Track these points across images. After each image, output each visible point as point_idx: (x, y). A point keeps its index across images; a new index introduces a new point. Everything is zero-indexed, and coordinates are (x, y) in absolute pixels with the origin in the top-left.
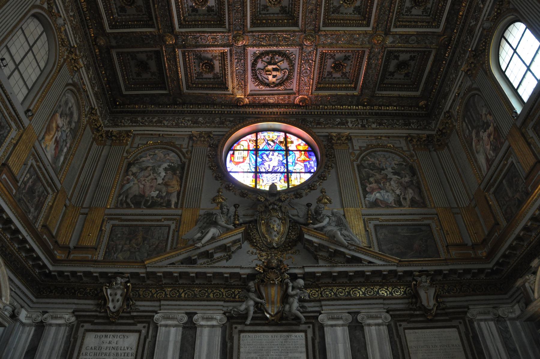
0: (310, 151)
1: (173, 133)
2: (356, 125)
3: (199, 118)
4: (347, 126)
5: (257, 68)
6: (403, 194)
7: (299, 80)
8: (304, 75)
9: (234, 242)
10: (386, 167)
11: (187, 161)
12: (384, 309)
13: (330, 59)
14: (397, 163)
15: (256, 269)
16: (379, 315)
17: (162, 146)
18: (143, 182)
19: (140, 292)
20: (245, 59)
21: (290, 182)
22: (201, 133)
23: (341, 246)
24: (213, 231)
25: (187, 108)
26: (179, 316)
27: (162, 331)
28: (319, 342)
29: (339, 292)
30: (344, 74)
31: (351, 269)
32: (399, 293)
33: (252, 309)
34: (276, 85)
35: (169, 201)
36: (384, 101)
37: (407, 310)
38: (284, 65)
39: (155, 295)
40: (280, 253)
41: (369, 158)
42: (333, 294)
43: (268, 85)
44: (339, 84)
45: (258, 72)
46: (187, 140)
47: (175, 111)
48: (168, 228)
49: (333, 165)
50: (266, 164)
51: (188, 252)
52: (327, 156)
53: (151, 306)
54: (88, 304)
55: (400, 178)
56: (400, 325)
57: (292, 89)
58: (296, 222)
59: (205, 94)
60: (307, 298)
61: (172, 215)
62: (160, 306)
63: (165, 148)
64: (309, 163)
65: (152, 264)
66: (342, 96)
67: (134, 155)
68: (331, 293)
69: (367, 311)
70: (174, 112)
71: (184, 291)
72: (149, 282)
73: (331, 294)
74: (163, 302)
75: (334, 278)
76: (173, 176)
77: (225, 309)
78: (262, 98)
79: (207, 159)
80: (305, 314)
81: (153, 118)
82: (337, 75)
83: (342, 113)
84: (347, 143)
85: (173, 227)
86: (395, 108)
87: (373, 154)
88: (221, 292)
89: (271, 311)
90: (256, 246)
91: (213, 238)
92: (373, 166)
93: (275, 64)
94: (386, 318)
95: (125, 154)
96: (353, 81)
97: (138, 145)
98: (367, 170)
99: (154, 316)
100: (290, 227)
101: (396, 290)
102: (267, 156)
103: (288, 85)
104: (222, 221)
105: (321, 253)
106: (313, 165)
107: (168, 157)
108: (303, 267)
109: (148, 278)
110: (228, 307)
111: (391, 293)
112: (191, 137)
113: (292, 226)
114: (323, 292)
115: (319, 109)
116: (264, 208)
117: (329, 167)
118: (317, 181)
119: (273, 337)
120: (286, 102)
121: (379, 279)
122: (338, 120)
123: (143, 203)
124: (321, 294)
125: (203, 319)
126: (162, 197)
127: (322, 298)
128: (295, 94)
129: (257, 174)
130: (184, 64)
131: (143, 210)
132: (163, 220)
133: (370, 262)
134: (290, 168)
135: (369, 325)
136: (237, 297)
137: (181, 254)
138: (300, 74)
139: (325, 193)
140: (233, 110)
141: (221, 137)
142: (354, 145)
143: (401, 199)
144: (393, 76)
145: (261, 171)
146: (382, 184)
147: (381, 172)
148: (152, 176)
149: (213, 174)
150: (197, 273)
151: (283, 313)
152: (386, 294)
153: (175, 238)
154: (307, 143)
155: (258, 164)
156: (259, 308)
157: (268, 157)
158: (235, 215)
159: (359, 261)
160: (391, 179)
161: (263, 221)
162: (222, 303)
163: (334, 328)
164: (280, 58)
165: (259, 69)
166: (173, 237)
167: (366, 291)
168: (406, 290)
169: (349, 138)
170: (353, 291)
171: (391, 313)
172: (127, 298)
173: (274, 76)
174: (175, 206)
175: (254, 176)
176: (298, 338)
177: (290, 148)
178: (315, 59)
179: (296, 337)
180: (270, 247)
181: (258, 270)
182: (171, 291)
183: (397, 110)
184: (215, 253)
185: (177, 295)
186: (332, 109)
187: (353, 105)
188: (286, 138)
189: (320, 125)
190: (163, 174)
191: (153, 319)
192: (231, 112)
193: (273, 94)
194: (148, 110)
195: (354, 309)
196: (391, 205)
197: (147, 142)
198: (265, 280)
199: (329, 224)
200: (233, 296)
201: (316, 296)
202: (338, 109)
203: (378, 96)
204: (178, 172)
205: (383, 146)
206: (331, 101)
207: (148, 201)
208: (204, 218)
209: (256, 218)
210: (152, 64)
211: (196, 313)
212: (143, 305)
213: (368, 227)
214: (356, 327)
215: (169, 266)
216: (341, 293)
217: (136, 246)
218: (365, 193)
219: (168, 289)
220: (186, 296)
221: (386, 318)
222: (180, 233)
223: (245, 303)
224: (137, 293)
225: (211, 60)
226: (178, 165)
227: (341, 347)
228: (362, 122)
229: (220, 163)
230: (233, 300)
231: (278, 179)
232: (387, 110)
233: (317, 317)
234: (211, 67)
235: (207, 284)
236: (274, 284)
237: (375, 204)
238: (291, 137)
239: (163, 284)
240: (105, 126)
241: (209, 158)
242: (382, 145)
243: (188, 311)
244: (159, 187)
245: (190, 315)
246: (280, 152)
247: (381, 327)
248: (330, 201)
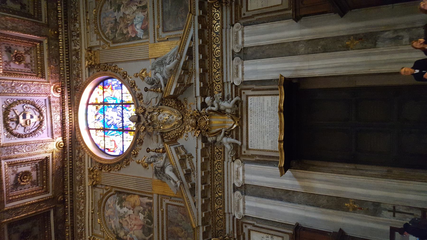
1: (91, 201)
2: (78, 41)
3: (77, 180)
4: (79, 50)
5: (23, 133)
6: (136, 4)
7: (35, 94)
8: (28, 90)
9: (178, 152)
10: (114, 18)
11: (114, 189)
12: (230, 28)
13: (10, 65)
14: (109, 7)
15: (197, 136)
16: (235, 33)
17: (102, 210)
18: (132, 226)
19: (219, 230)
20: (14, 145)
21: (130, 102)
22: (90, 178)
23: (179, 64)
24: (168, 171)
25: (67, 191)
26: (236, 198)
27: (248, 213)
28: (256, 85)
29: (217, 67)
30: (27, 52)
32: (218, 14)
33: (230, 140)
34: (41, 114)
35: (147, 204)
36: (52, 15)
37: (232, 8)
38: (19, 109)
39: (221, 217)
40: (186, 114)
41: (107, 32)
42: (218, 72)
43: (41, 122)
44: (37, 57)
45: (28, 132)
46: (97, 190)
47: (70, 200)
48: (168, 205)
49: (113, 65)
50: (116, 121)
51: (185, 191)
52: (107, 70)
53: (229, 220)
55: (122, 6)
56: (244, 14)
57: (45, 100)
58: (162, 100)
59: (52, 177)
60: (221, 94)
61: (158, 202)
62: (229, 213)
63: (104, 207)
64: (114, 85)
65: (196, 221)
66: (49, 55)
67: (110, 235)
68: (217, 74)
69: (232, 44)
70: (72, 201)
71: (217, 193)
72: (210, 222)
73: (218, 74)
74: (226, 211)
75: (205, 71)
76: (128, 201)
77: (230, 160)
78: (56, 126)
79: (112, 172)
80: (234, 96)
81: (78, 219)
82: (28, 59)
83: (67, 54)
84: (94, 52)
85: (167, 201)
86: (59, 4)
87: (103, 28)
88: (217, 163)
89: (231, 124)
90: (181, 133)
91: (174, 171)
92: (114, 29)
93: (18, 117)
94: (238, 27)
96: (33, 44)
97: (102, 231)
98: (116, 35)
99: (237, 219)
100: (165, 105)
101: (215, 17)
102: (109, 120)
103: (39, 104)
104: (160, 162)
105: (186, 81)
106: (115, 82)
107: (111, 205)
108: (196, 97)
109: (208, 223)
110: (228, 158)
111: (218, 21)
112: (94, 186)
113: (165, 103)
114: (216, 80)
115: (64, 75)
116: (150, 127)
117: (115, 69)
118: (128, 79)
119: (251, 122)
120: (59, 104)
121: (206, 31)
122: (74, 58)
123: (149, 226)
124: (218, 82)
125: (238, 178)
126: (144, 210)
127: (221, 81)
128: (49, 97)
129: (124, 130)
130: (22, 200)
131: (154, 226)
132: (162, 210)
133: (192, 40)
134: (119, 102)
135: (243, 42)
136: (221, 150)
137: (187, 197)
138: (27, 94)
139: (137, 73)
140: (68, 151)
141: (93, 161)
142: (95, 45)
143: (140, 5)
144: (25, 5)
145: (121, 126)
146: (129, 22)
147: (118, 23)
148: (127, 218)
149: (124, 167)
150: (202, 184)
151: (232, 114)
152: (219, 26)
153: (177, 199)
154: (97, 86)
155: (116, 129)
156: (229, 133)
157: (110, 120)
158: (155, 152)
160: (124, 13)
161: (161, 127)
162: (225, 163)
163: (244, 73)
164: (12, 113)
165: (24, 131)
166: (175, 201)
167: (216, 43)
168: (215, 8)
169: (90, 49)
170: (216, 55)
171: (233, 23)
173: (32, 117)
174: (151, 199)
175: (126, 132)
177: (102, 101)
178: (10, 80)
179: (251, 104)
181: (198, 134)
182: (217, 204)
183: (61, 3)
184: (186, 168)
185: (220, 199)
186: (64, 63)
187: (59, 44)
188: (93, 104)
189: (79, 75)
190: (125, 209)
191: (239, 220)
192: (70, 152)
193: (51, 117)
194: (71, 224)
195: (230, 55)
196: (146, 16)
197: (99, 223)
198: (207, 129)
199: (161, 73)
200: (220, 153)
201: (219, 86)
202: (63, 58)
203: (48, 20)
204: (123, 197)
205: (96, 19)
206: (55, 65)
207: (147, 222)
208: (159, 176)
209: (159, 133)
210: (24, 227)
211: (234, 184)
212: (229, 227)
213: (164, 38)
214: (245, 54)
215: (196, 207)
216: (217, 65)
217: (183, 233)
218: (136, 38)
219: (216, 206)
220: (221, 192)
221: (238, 27)
222: (172, 195)
223: (225, 145)
224: (220, 232)
225: (18, 175)
226: (117, 196)
227: (260, 68)
228: (75, 36)
229: (115, 161)
230: (223, 153)
231: (128, 112)
232: (61, 12)
233: (236, 86)
234: (26, 173)
235: (211, 175)
236: (209, 121)
237: (145, 30)
238: (92, 100)
239: (212, 211)
241: (111, 170)
242: (95, 19)
243: (232, 190)
244: (136, 212)
245: (235, 189)
246: (105, 109)
247: (245, 31)
248: (144, 70)
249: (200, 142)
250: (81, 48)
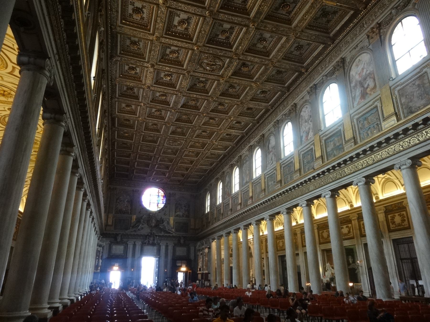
0: (165, 196)
27: (129, 245)
31: (168, 235)
89: (151, 242)
156: (149, 241)
159: (170, 233)
172: (121, 239)
176: (155, 248)
180: (151, 226)
190: (126, 203)
195: (167, 242)
212: (125, 240)
218: (176, 212)
237: (177, 216)
245: (135, 242)
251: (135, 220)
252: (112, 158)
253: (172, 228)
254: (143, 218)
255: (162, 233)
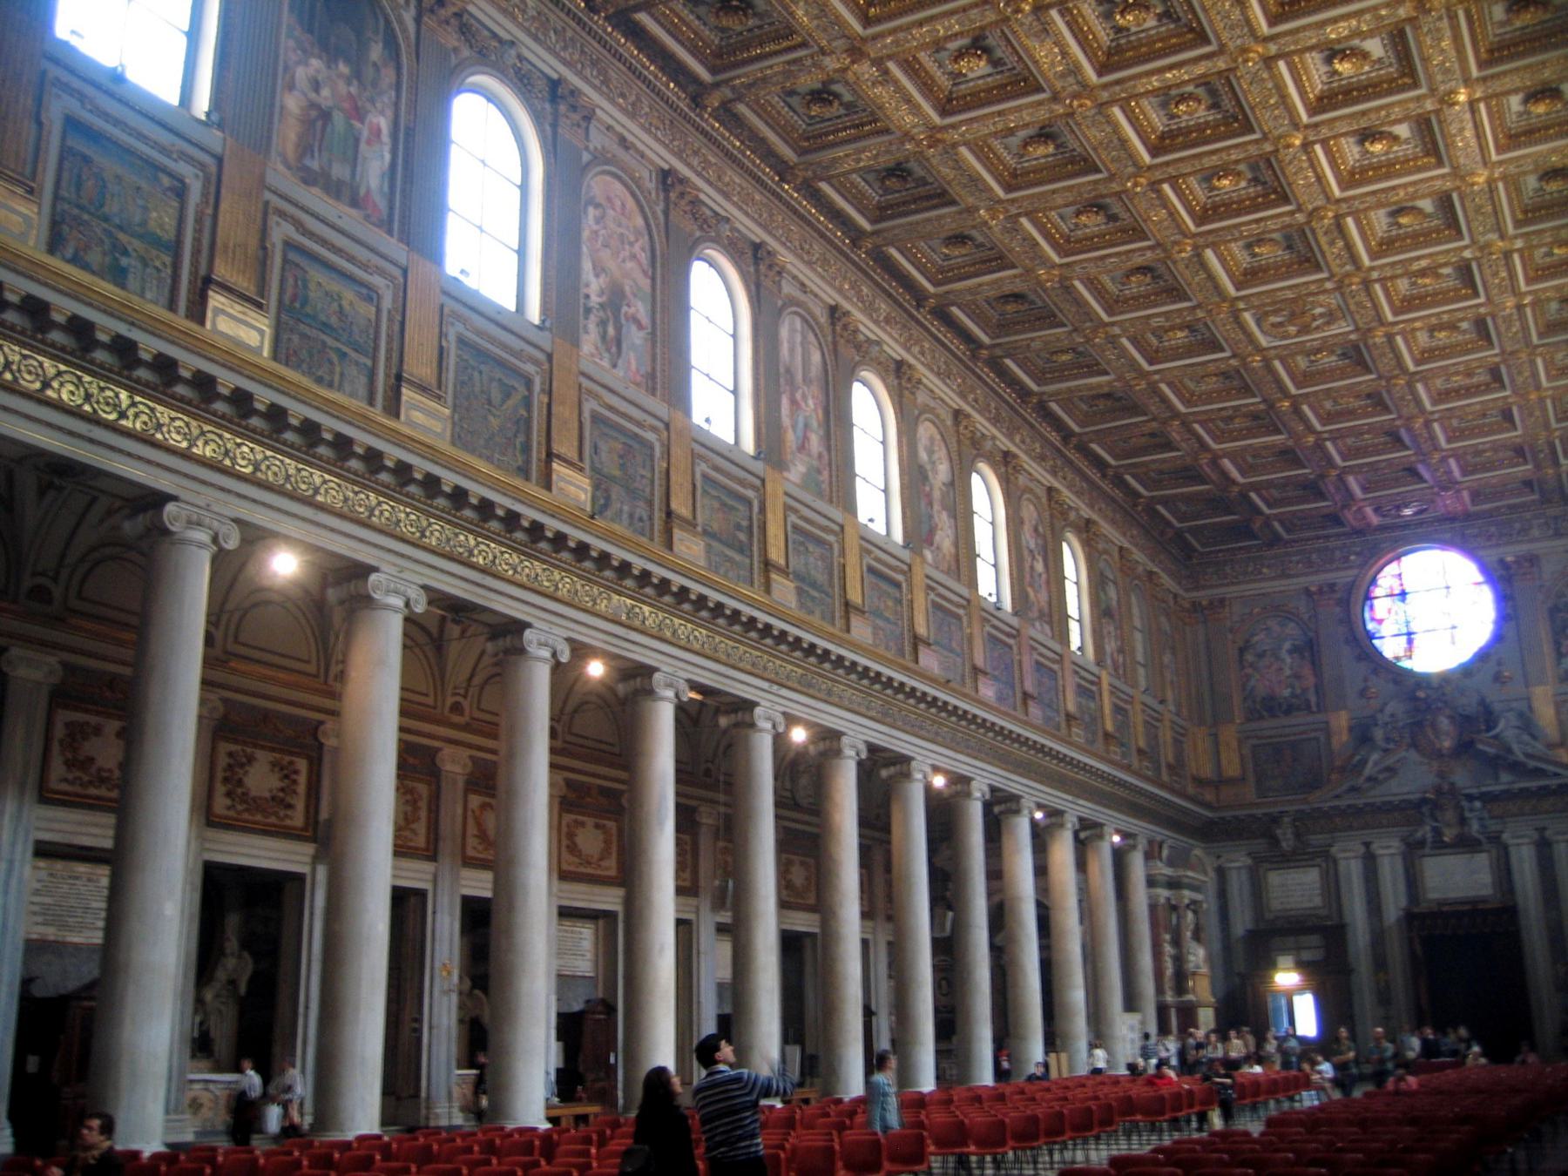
27: (1342, 865)
35: (1308, 702)
54: (1260, 845)
95: (1230, 636)
122: (1517, 526)
133: (1556, 775)
156: (1437, 832)
169: (1532, 560)
172: (1298, 835)
176: (1482, 860)
180: (1439, 755)
190: (1289, 660)
212: (1316, 839)
233: (1498, 838)
240: (1187, 590)
245: (1367, 845)
249: (1418, 796)
250: (1532, 541)
251: (1345, 737)
252: (1104, 476)
253: (1550, 746)
254: (1382, 718)
255: (1505, 777)
